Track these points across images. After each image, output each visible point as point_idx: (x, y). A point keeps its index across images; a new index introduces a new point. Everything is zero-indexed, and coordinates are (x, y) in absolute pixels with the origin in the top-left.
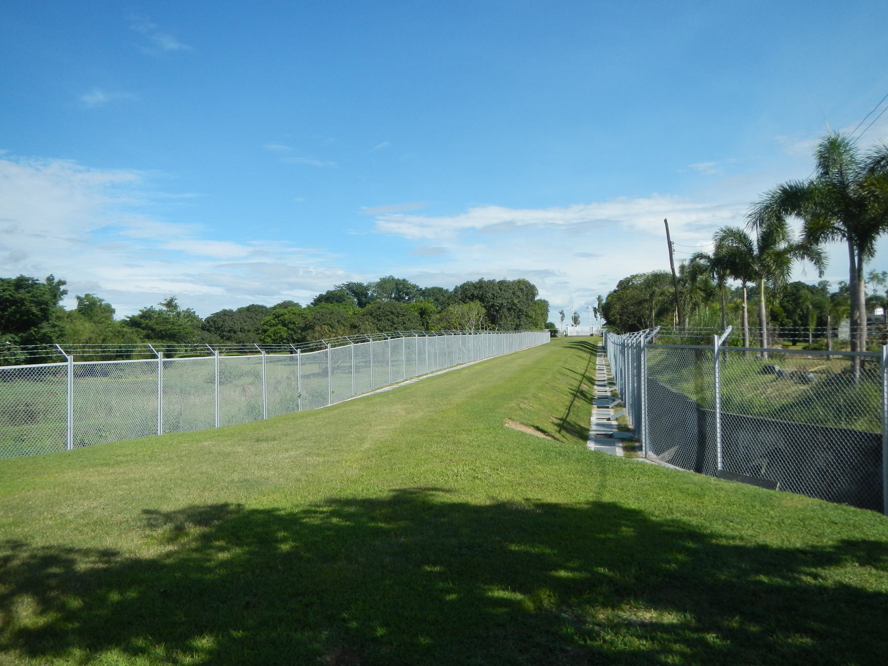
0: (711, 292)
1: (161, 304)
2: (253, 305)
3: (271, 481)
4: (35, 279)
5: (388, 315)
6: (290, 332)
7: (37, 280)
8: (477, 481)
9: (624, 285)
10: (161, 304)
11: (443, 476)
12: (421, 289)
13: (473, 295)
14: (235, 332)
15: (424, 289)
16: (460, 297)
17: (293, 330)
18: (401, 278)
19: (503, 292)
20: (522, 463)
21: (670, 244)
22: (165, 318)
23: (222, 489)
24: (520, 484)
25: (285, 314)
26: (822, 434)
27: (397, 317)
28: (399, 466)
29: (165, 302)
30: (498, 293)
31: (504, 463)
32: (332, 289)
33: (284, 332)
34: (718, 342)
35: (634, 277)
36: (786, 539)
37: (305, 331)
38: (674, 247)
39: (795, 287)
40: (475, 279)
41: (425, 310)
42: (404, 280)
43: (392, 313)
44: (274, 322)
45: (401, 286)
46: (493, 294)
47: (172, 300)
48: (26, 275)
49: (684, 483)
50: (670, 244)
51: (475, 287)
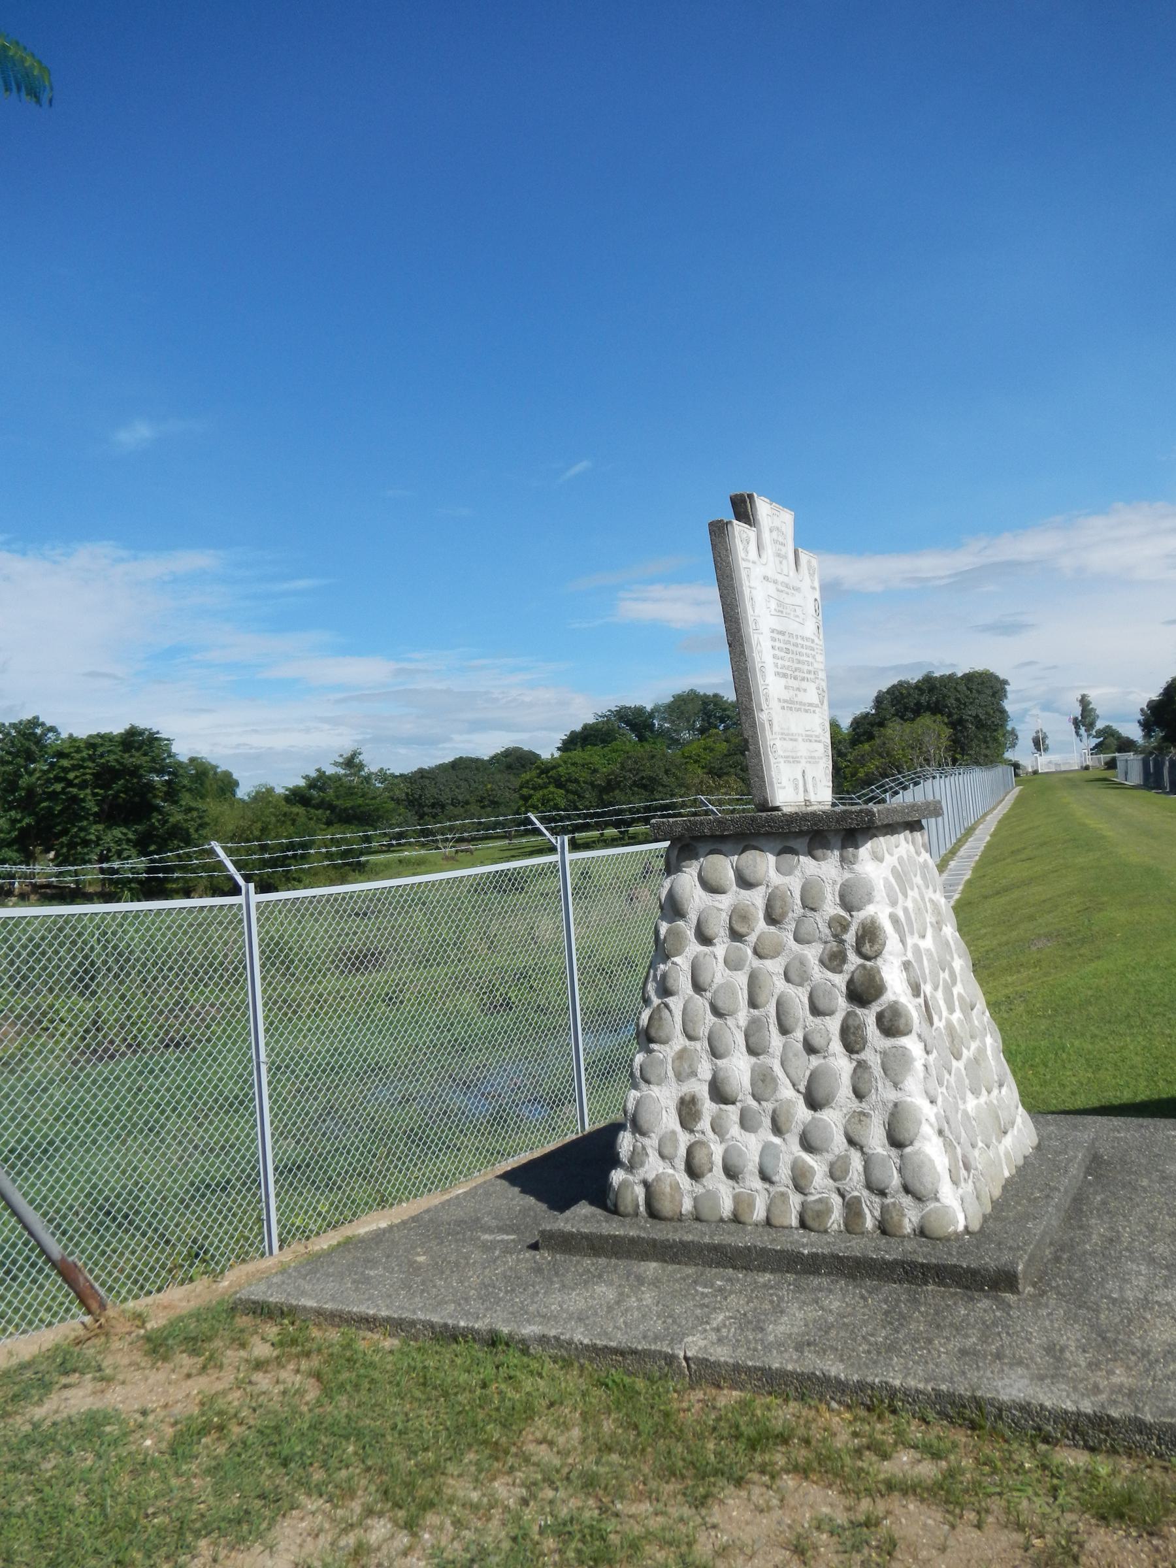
1: (336, 764)
4: (155, 730)
6: (571, 797)
7: (158, 733)
10: (336, 764)
13: (918, 704)
14: (443, 807)
17: (575, 793)
18: (710, 693)
19: (975, 694)
22: (350, 788)
25: (560, 766)
29: (341, 760)
30: (967, 697)
32: (591, 720)
37: (607, 793)
40: (914, 677)
42: (716, 696)
44: (540, 781)
45: (711, 707)
46: (957, 700)
47: (355, 755)
48: (142, 724)
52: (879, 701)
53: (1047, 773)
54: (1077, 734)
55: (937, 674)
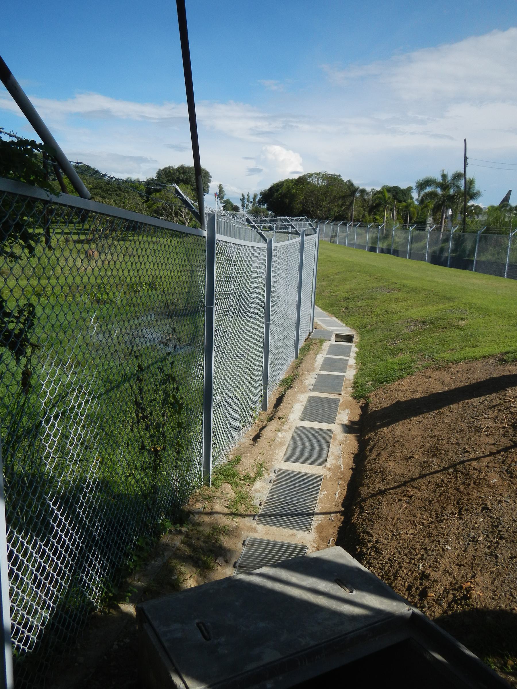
13: (178, 178)
21: (466, 158)
35: (311, 175)
38: (468, 161)
39: (395, 190)
50: (466, 158)
52: (160, 174)
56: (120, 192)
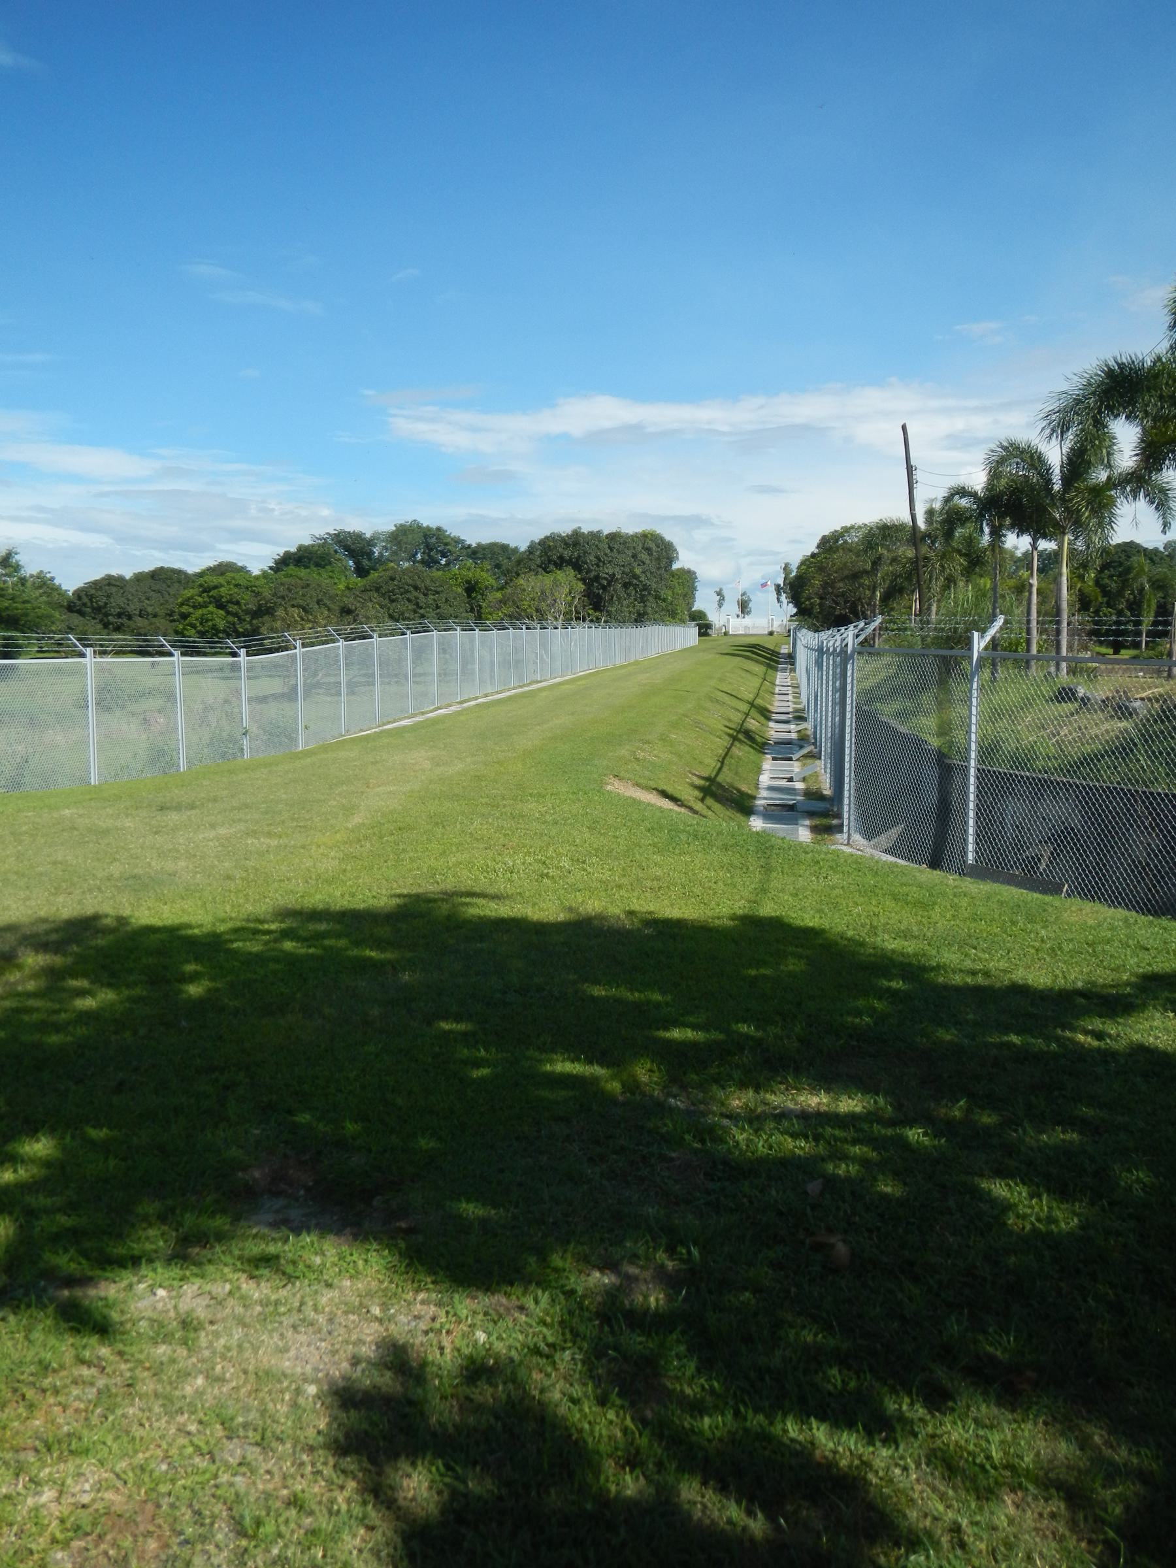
0: (978, 557)
2: (162, 568)
3: (180, 878)
5: (408, 591)
6: (231, 618)
8: (545, 880)
9: (829, 544)
11: (488, 872)
12: (469, 546)
13: (561, 558)
14: (130, 618)
15: (474, 545)
16: (538, 561)
17: (236, 615)
18: (433, 525)
19: (615, 554)
20: (628, 851)
21: (910, 469)
23: (90, 891)
24: (620, 887)
25: (222, 586)
26: (1143, 802)
27: (425, 595)
28: (412, 854)
30: (606, 555)
31: (597, 850)
32: (307, 542)
33: (220, 619)
34: (979, 644)
35: (846, 530)
36: (1060, 975)
37: (257, 618)
38: (918, 475)
39: (1125, 551)
40: (565, 529)
41: (476, 583)
42: (439, 529)
43: (416, 588)
44: (200, 599)
45: (433, 540)
46: (598, 558)
47: (9, 555)
49: (902, 885)
51: (566, 544)
53: (735, 635)
54: (778, 600)
55: (585, 530)
56: (416, 594)
